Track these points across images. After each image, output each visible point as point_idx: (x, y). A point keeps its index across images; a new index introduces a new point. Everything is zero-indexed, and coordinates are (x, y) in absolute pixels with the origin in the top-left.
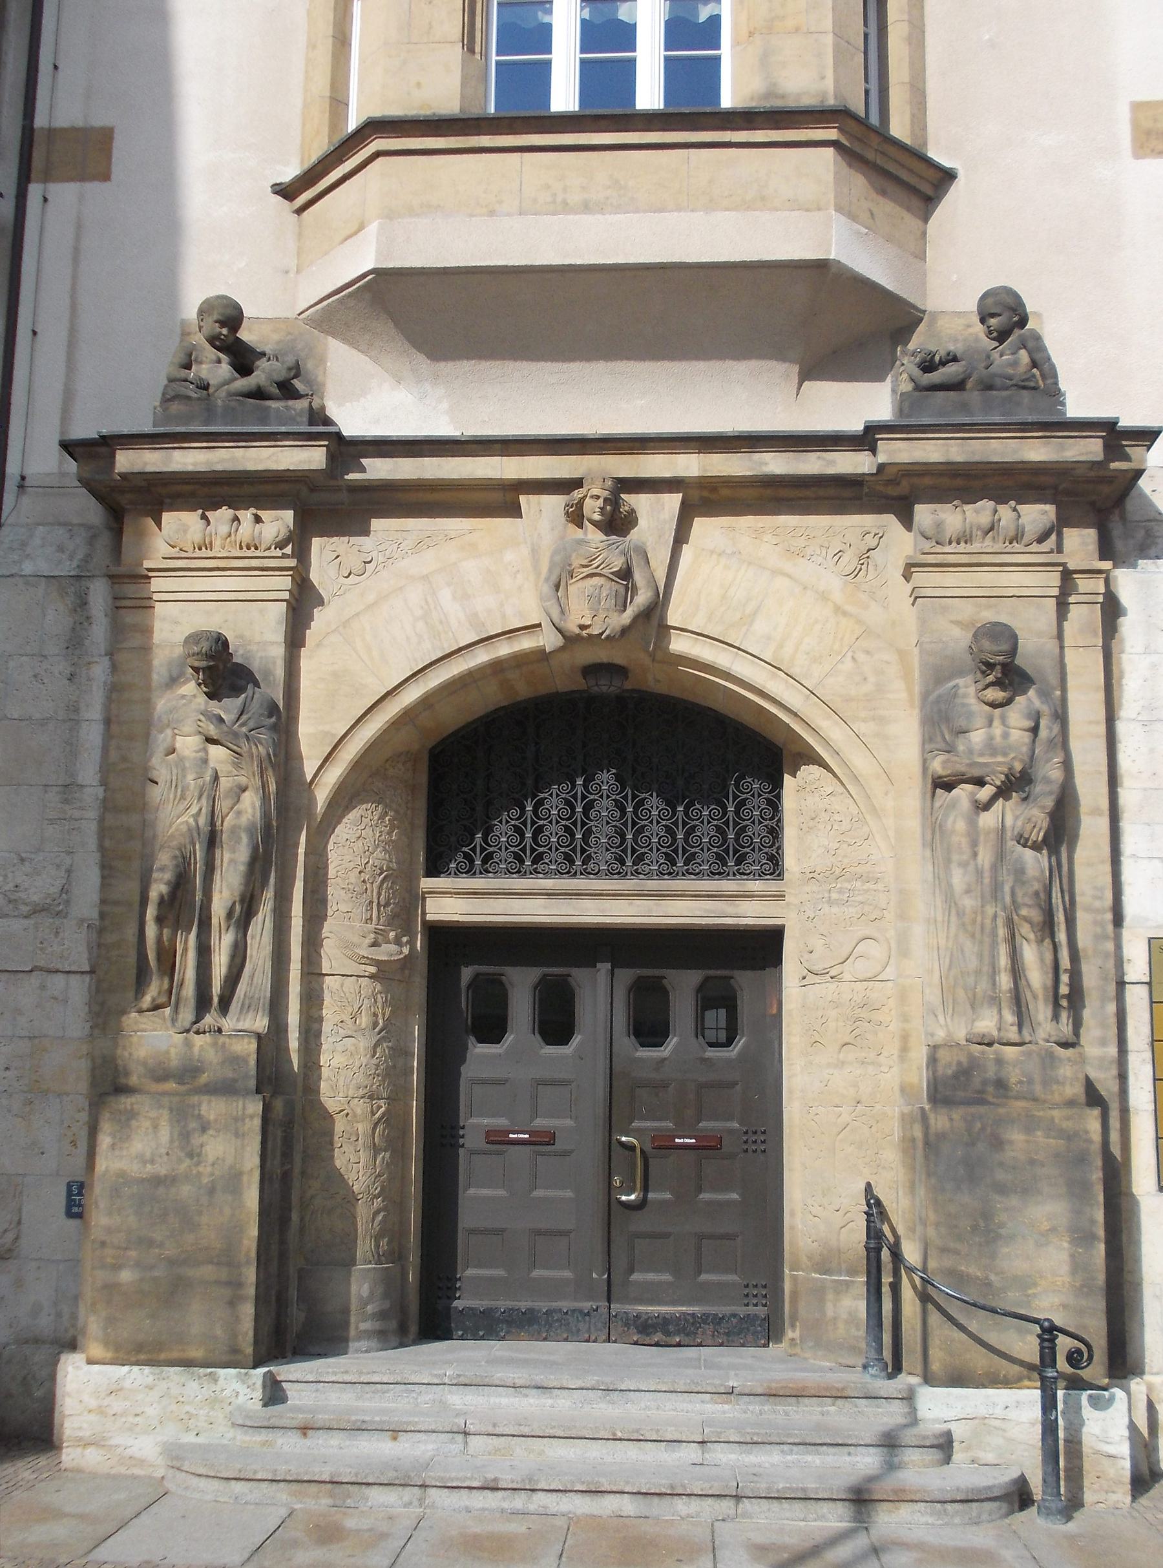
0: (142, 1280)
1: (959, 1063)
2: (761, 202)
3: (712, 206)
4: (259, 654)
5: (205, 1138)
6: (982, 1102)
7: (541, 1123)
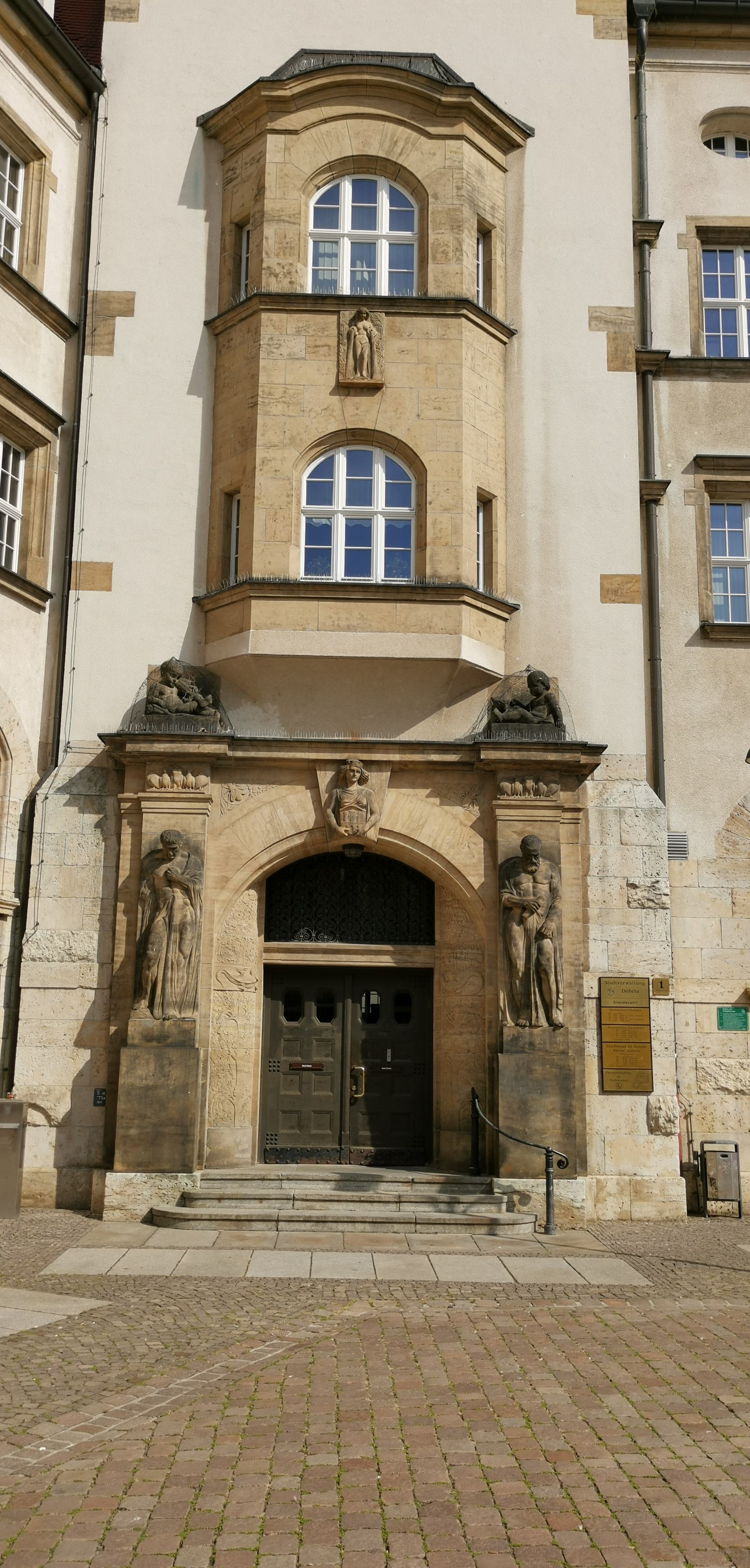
1: (513, 1035)
2: (429, 629)
3: (406, 630)
5: (170, 1068)
6: (523, 1052)
7: (315, 1059)
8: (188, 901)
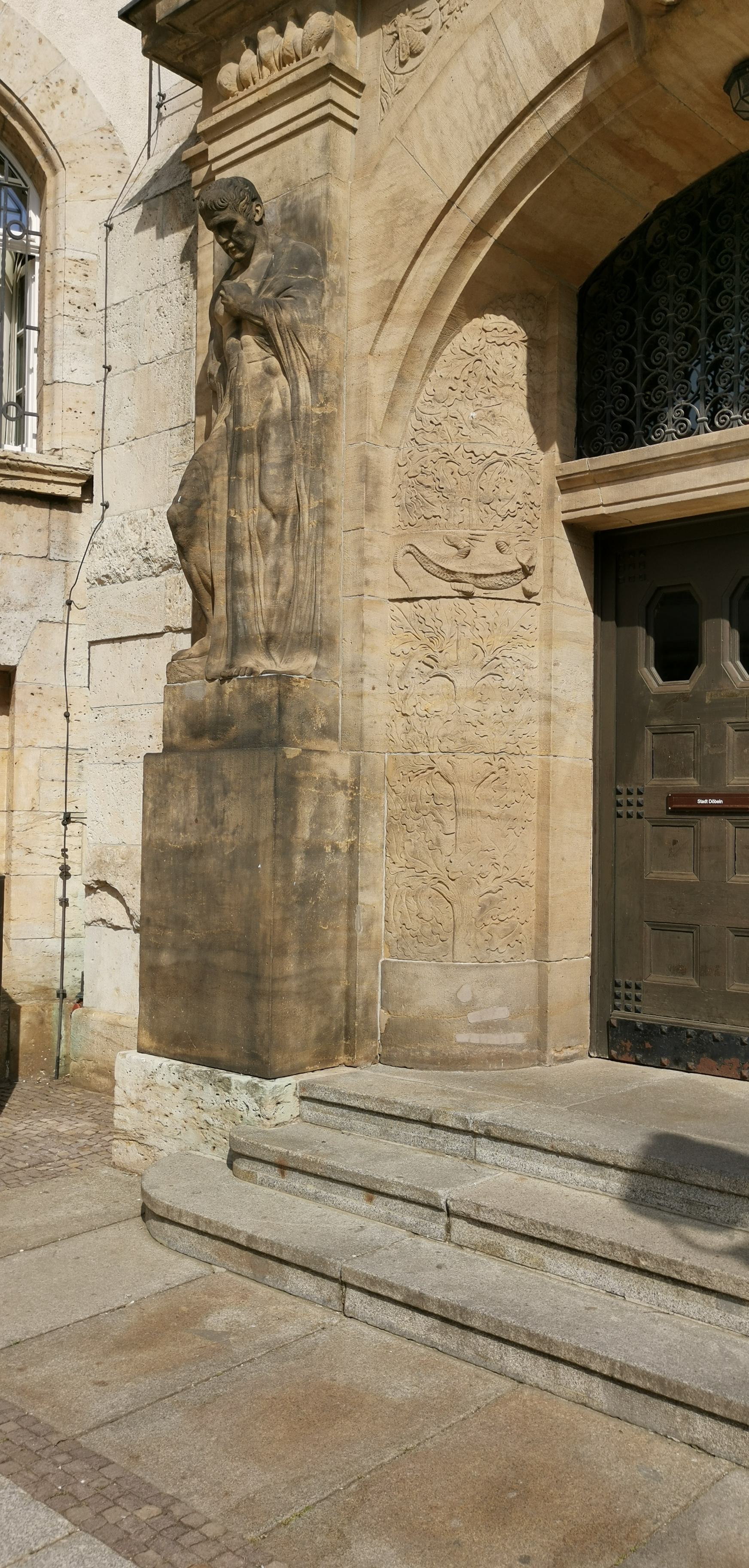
0: (177, 964)
4: (305, 199)
8: (274, 362)
